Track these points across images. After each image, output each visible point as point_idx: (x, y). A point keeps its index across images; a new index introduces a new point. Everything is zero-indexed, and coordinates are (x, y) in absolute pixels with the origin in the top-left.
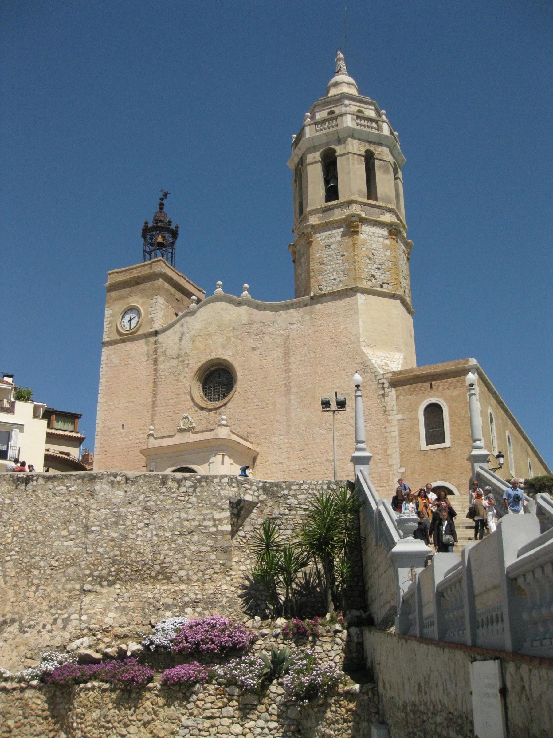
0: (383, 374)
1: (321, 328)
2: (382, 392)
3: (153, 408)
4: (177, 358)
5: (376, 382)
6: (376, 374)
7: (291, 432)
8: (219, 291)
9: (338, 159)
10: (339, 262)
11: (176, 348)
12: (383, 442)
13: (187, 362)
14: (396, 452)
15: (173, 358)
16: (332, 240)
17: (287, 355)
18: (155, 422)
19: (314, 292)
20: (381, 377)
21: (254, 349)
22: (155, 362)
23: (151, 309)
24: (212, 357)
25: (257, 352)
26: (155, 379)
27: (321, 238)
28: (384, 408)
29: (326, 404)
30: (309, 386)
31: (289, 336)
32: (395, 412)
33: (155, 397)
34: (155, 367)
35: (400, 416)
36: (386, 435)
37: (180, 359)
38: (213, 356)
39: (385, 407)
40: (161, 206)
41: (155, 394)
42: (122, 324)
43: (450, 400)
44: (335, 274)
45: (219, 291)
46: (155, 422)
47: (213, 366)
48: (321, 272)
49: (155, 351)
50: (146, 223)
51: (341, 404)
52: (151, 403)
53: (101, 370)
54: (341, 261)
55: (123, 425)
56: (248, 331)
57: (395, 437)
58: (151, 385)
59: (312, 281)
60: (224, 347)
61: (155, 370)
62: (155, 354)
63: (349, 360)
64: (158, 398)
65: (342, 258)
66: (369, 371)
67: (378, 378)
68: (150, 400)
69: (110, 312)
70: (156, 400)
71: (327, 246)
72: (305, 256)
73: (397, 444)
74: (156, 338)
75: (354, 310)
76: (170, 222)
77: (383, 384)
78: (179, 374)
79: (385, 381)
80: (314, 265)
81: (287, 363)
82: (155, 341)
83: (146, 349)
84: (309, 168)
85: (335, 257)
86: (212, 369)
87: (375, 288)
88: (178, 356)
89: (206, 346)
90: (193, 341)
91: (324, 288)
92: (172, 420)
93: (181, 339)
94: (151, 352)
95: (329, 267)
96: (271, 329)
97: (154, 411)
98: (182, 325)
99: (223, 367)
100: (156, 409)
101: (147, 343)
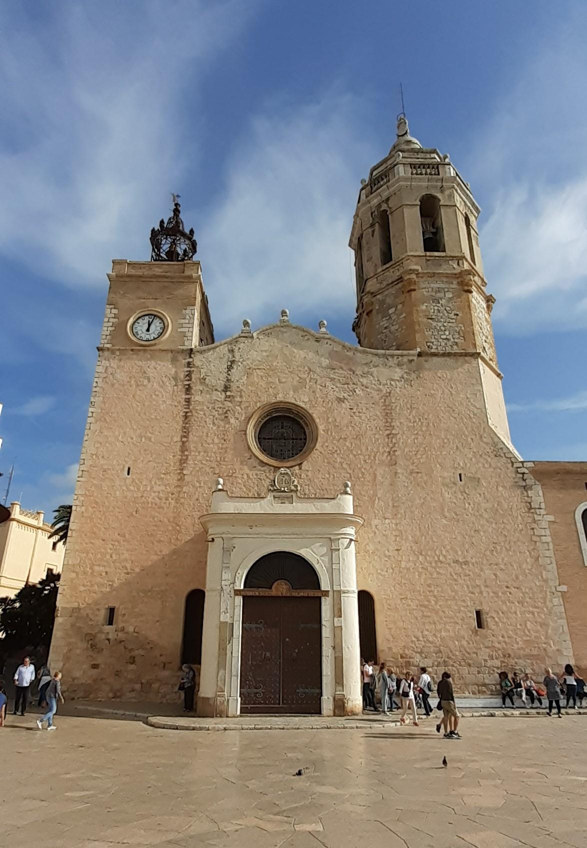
0: (522, 462)
1: (432, 392)
2: (524, 484)
3: (182, 451)
4: (223, 391)
5: (514, 470)
6: (513, 460)
7: (399, 516)
9: (442, 210)
10: (451, 321)
11: (223, 377)
12: (532, 547)
13: (238, 399)
14: (551, 563)
15: (216, 390)
16: (439, 295)
18: (185, 472)
19: (420, 348)
20: (521, 465)
21: (340, 400)
22: (188, 389)
23: (183, 321)
24: (278, 399)
25: (346, 405)
26: (186, 413)
27: (427, 290)
28: (528, 504)
30: (422, 461)
31: (390, 393)
32: (543, 512)
33: (185, 437)
34: (187, 397)
35: (551, 518)
36: (534, 538)
37: (228, 393)
38: (280, 397)
39: (530, 503)
40: (176, 211)
41: (186, 432)
42: (134, 331)
44: (447, 333)
46: (185, 472)
47: (276, 412)
48: (430, 328)
49: (189, 375)
50: (162, 222)
52: (180, 444)
53: (95, 384)
54: (454, 321)
55: (129, 469)
56: (332, 376)
57: (548, 543)
58: (180, 419)
59: (417, 335)
60: (295, 390)
61: (188, 401)
62: (188, 380)
63: (473, 437)
64: (190, 439)
65: (455, 317)
66: (503, 455)
67: (515, 465)
68: (179, 439)
69: (115, 311)
70: (187, 441)
72: (400, 307)
73: (550, 553)
74: (191, 360)
76: (192, 232)
77: (523, 474)
78: (226, 413)
79: (526, 471)
82: (189, 364)
83: (174, 370)
84: (406, 211)
85: (446, 314)
86: (274, 415)
88: (226, 388)
89: (268, 383)
90: (249, 375)
91: (434, 347)
92: (215, 474)
93: (230, 368)
94: (182, 376)
95: (440, 324)
96: (364, 381)
97: (184, 455)
98: (232, 351)
99: (292, 416)
100: (186, 453)
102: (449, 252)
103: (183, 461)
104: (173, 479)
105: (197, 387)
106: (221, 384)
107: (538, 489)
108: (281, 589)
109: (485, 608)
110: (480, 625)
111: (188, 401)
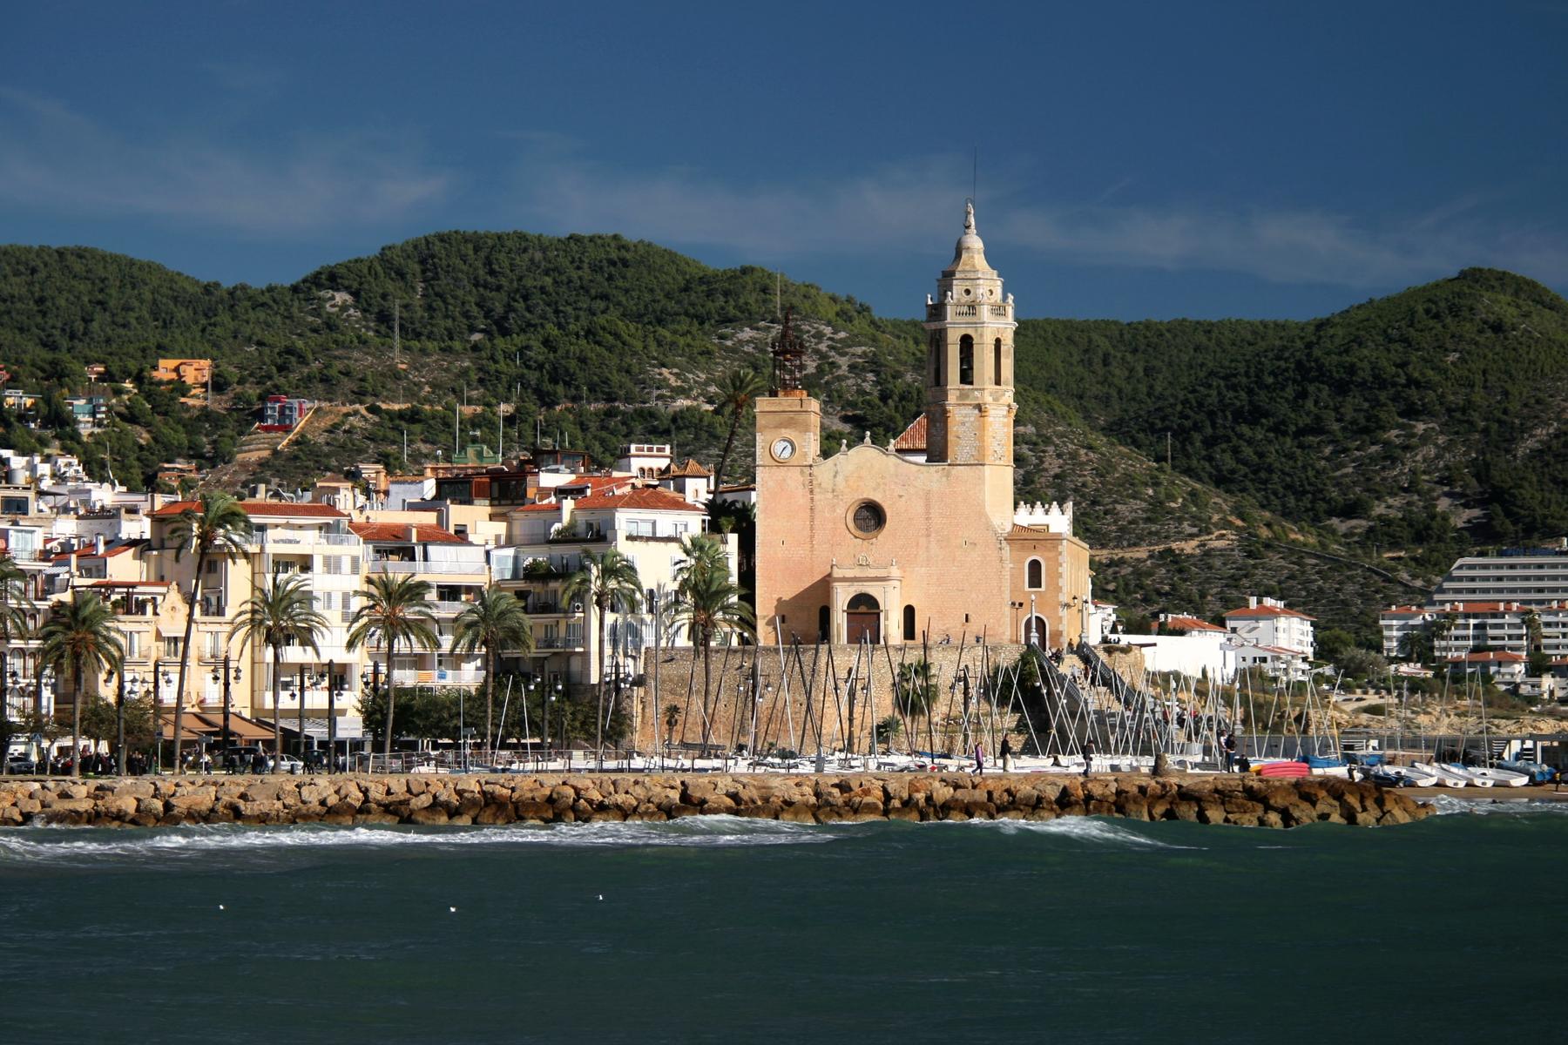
8: (868, 439)
17: (928, 506)
22: (811, 492)
29: (1013, 604)
38: (865, 496)
41: (812, 520)
43: (1047, 559)
45: (868, 439)
48: (957, 445)
51: (1021, 605)
60: (875, 490)
61: (812, 499)
71: (963, 424)
75: (981, 479)
80: (951, 437)
81: (928, 513)
84: (950, 347)
87: (997, 462)
88: (833, 491)
101: (802, 472)
102: (974, 387)
103: (812, 537)
104: (808, 547)
105: (817, 490)
106: (830, 488)
107: (1008, 548)
108: (863, 609)
109: (970, 613)
110: (967, 620)
111: (812, 499)
